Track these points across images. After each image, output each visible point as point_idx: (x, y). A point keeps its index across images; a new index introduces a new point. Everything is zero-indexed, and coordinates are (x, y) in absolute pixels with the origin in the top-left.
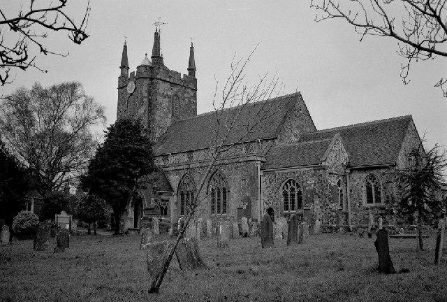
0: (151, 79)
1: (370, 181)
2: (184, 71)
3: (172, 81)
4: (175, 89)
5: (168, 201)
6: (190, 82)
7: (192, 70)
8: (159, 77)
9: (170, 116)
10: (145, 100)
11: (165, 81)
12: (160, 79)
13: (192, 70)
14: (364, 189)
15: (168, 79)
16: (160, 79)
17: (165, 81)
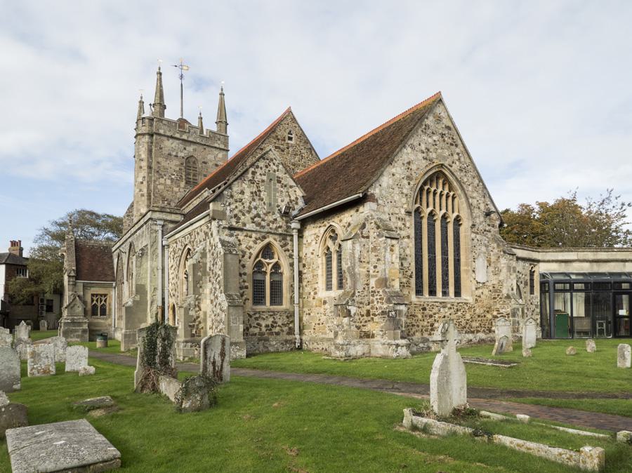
0: (151, 135)
1: (330, 243)
2: (210, 125)
3: (185, 137)
4: (191, 148)
5: (105, 295)
6: (219, 138)
7: (222, 121)
8: (161, 132)
9: (183, 184)
10: (144, 164)
11: (172, 137)
12: (164, 136)
13: (222, 121)
14: (321, 261)
15: (177, 135)
16: (164, 136)
17: (172, 137)
